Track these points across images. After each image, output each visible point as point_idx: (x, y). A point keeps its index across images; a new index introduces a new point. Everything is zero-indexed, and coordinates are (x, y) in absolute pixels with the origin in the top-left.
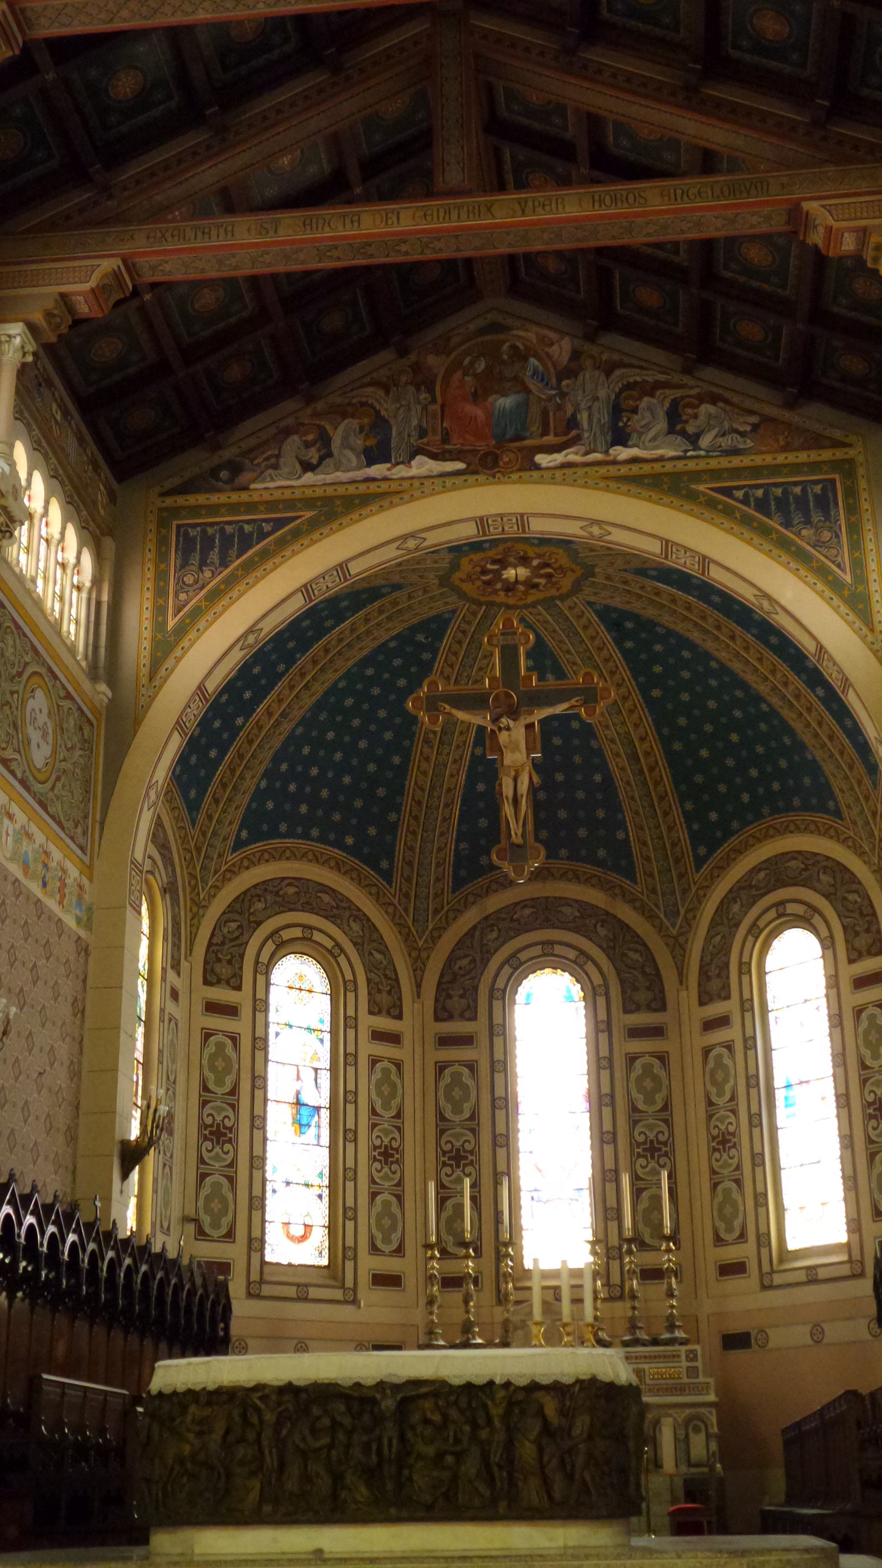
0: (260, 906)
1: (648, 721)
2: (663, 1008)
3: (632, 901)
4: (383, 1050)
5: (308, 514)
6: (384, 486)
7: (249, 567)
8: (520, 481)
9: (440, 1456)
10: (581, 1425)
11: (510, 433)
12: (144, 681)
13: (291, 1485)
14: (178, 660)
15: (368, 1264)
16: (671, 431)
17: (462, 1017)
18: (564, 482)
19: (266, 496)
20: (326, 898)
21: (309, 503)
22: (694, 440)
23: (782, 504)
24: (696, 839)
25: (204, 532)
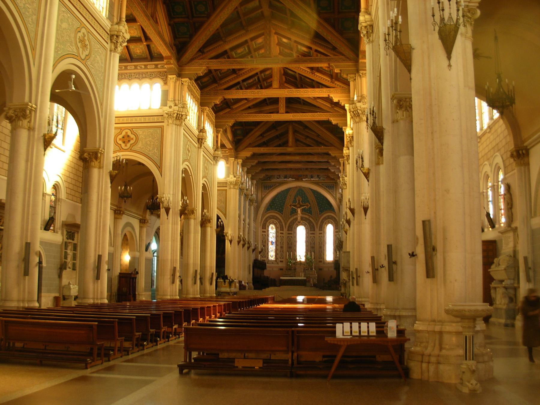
2: (315, 231)
3: (312, 217)
4: (281, 235)
7: (271, 190)
15: (279, 259)
16: (318, 177)
21: (278, 183)
22: (320, 178)
24: (320, 211)
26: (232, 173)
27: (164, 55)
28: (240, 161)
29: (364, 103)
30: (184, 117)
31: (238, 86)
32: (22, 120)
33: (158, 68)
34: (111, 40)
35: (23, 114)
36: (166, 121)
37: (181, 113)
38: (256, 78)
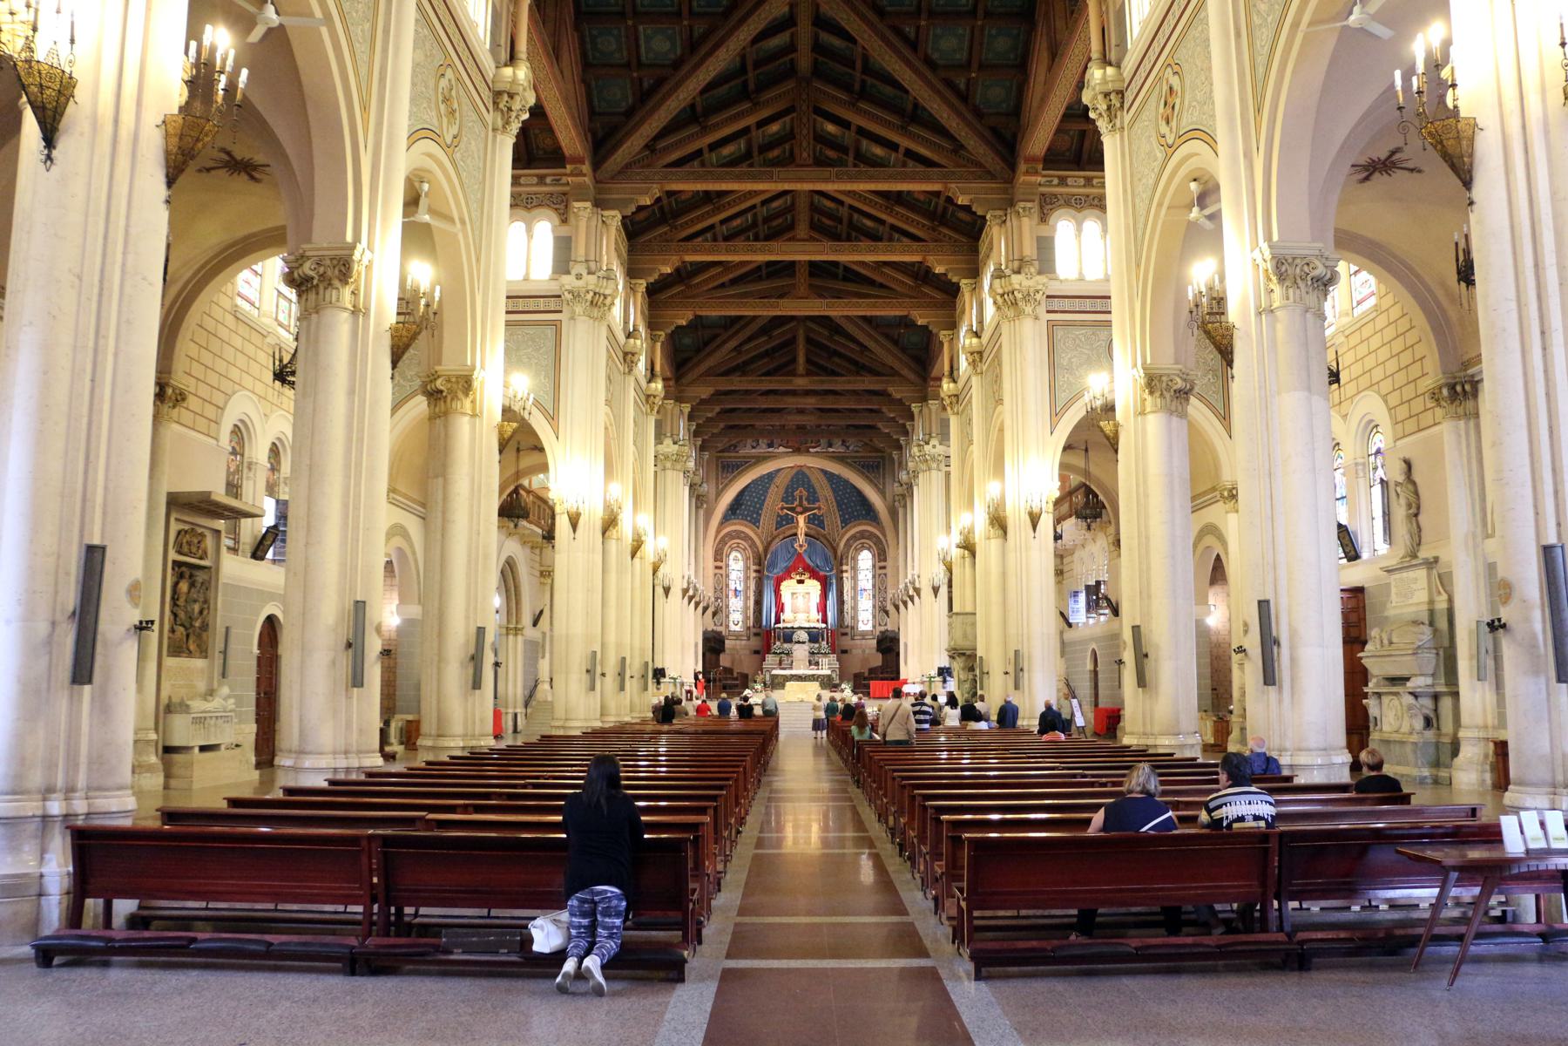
1: (831, 494)
7: (739, 474)
21: (753, 457)
22: (848, 448)
26: (669, 435)
27: (567, 152)
28: (687, 408)
29: (1029, 276)
30: (608, 301)
31: (709, 235)
32: (337, 288)
33: (546, 184)
34: (495, 103)
35: (340, 271)
36: (565, 309)
37: (602, 292)
38: (749, 216)
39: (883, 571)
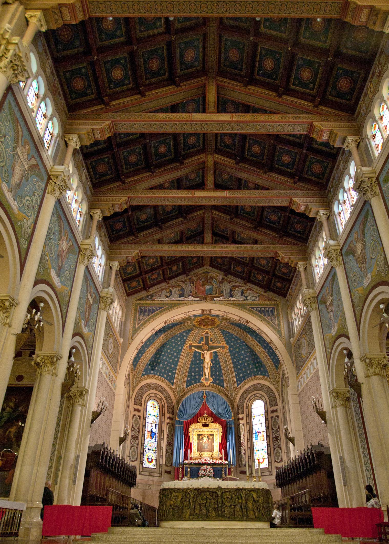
0: (146, 388)
5: (167, 306)
6: (183, 302)
7: (154, 316)
8: (211, 303)
9: (231, 506)
10: (261, 500)
11: (209, 293)
12: (130, 338)
13: (197, 511)
14: (138, 334)
15: (165, 468)
17: (275, 406)
18: (220, 304)
19: (158, 302)
20: (159, 387)
21: (167, 304)
22: (246, 297)
23: (264, 311)
24: (237, 380)
25: (145, 309)
39: (275, 414)
